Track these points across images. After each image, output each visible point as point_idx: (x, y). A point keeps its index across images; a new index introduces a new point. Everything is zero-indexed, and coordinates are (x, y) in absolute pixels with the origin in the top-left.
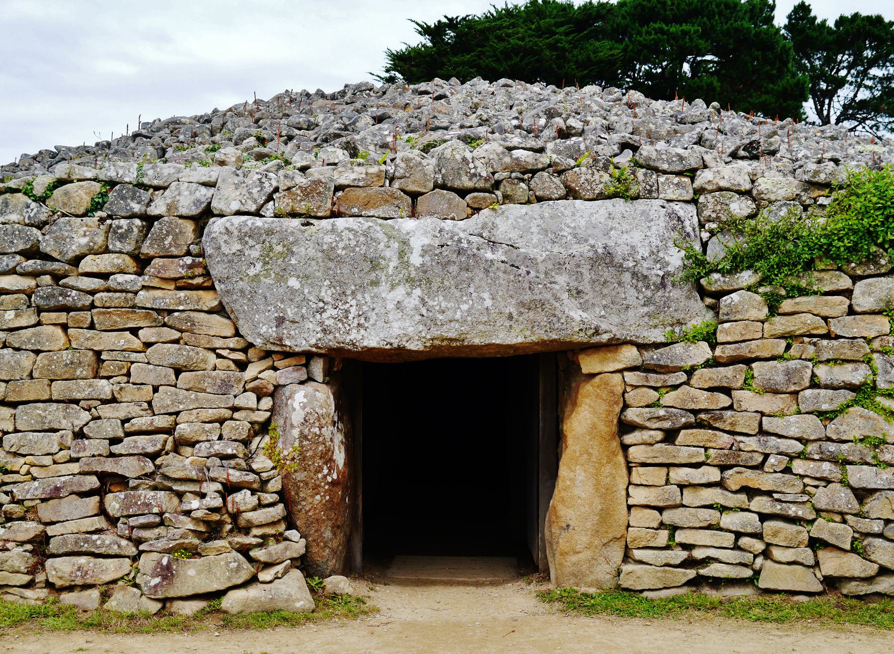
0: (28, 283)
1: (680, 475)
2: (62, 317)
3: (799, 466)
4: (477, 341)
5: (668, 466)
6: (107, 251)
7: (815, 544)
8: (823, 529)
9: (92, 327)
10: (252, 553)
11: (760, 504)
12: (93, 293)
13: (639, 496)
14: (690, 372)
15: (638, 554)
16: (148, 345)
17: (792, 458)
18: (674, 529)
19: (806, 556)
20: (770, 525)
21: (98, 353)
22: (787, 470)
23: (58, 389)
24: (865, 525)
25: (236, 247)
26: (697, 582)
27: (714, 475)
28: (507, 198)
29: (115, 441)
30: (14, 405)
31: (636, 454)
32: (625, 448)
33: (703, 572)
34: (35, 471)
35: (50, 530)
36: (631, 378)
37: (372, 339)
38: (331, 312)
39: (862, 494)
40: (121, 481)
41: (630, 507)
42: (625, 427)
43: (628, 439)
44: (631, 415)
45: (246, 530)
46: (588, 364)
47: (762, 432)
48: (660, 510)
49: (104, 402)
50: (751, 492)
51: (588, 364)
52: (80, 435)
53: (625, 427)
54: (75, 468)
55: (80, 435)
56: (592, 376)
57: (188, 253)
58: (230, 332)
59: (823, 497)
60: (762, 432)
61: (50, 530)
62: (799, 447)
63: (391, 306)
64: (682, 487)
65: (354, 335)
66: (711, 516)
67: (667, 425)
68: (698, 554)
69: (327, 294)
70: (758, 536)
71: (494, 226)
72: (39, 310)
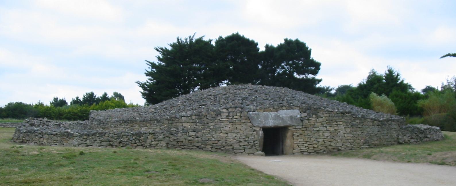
0: (228, 120)
1: (299, 140)
2: (232, 123)
3: (312, 139)
6: (236, 116)
7: (314, 147)
8: (315, 146)
9: (235, 124)
10: (257, 149)
11: (308, 143)
12: (235, 120)
13: (295, 143)
14: (300, 129)
15: (295, 149)
16: (242, 126)
17: (311, 138)
18: (298, 146)
19: (313, 148)
20: (309, 145)
21: (236, 128)
22: (311, 139)
23: (233, 131)
24: (318, 145)
25: (253, 115)
26: (301, 152)
27: (303, 140)
28: (281, 110)
29: (240, 137)
30: (227, 133)
31: (295, 138)
32: (293, 137)
33: (302, 150)
34: (231, 141)
35: (234, 147)
36: (294, 129)
37: (268, 126)
38: (264, 122)
39: (318, 142)
40: (241, 141)
42: (293, 135)
43: (294, 136)
44: (294, 134)
46: (290, 128)
47: (308, 135)
48: (297, 144)
49: (238, 133)
50: (307, 142)
52: (236, 136)
53: (293, 135)
54: (235, 140)
55: (236, 136)
56: (290, 129)
57: (246, 116)
58: (251, 125)
59: (314, 142)
60: (308, 135)
61: (234, 147)
62: (312, 137)
63: (270, 122)
64: (300, 141)
66: (303, 144)
67: (298, 135)
68: (301, 149)
69: (263, 120)
70: (307, 146)
72: (229, 122)
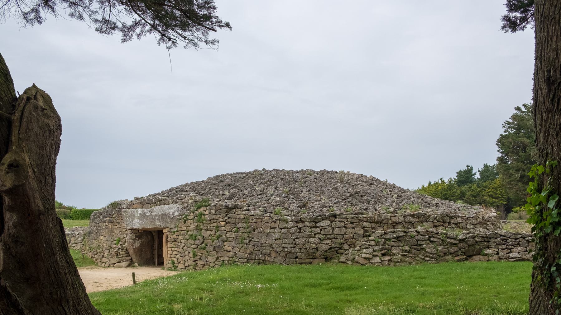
4: (146, 227)
5: (172, 248)
28: (156, 205)
41: (168, 254)
43: (168, 243)
45: (120, 255)
51: (164, 231)
64: (173, 251)
65: (133, 227)
71: (153, 209)
